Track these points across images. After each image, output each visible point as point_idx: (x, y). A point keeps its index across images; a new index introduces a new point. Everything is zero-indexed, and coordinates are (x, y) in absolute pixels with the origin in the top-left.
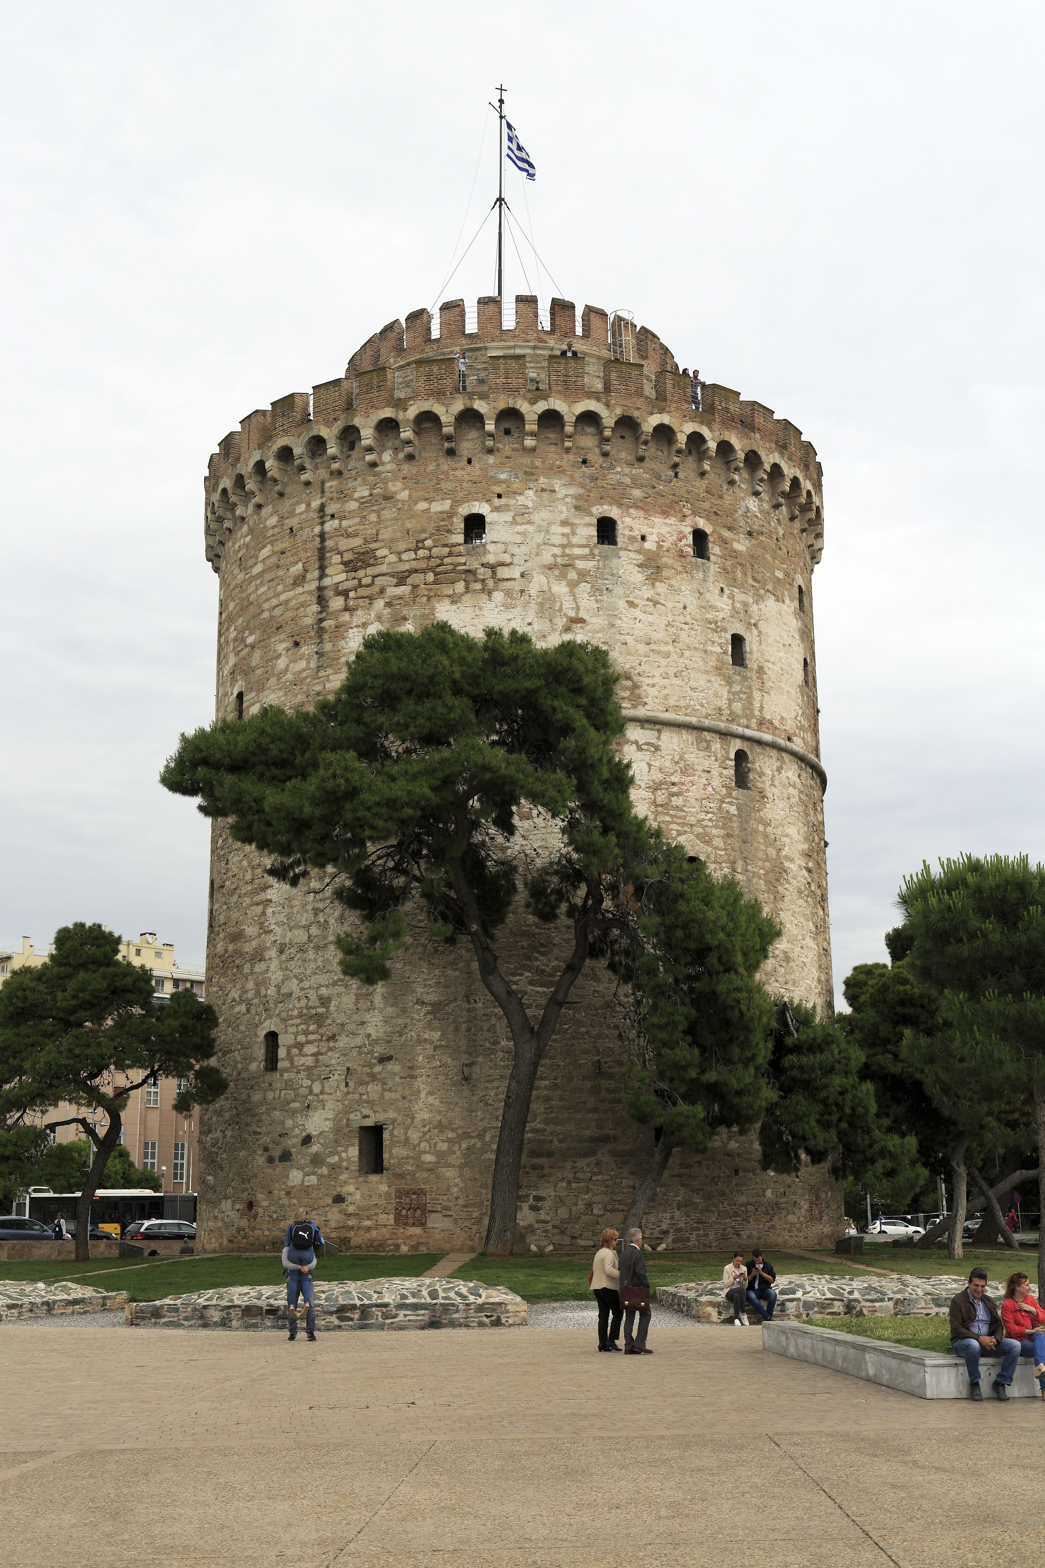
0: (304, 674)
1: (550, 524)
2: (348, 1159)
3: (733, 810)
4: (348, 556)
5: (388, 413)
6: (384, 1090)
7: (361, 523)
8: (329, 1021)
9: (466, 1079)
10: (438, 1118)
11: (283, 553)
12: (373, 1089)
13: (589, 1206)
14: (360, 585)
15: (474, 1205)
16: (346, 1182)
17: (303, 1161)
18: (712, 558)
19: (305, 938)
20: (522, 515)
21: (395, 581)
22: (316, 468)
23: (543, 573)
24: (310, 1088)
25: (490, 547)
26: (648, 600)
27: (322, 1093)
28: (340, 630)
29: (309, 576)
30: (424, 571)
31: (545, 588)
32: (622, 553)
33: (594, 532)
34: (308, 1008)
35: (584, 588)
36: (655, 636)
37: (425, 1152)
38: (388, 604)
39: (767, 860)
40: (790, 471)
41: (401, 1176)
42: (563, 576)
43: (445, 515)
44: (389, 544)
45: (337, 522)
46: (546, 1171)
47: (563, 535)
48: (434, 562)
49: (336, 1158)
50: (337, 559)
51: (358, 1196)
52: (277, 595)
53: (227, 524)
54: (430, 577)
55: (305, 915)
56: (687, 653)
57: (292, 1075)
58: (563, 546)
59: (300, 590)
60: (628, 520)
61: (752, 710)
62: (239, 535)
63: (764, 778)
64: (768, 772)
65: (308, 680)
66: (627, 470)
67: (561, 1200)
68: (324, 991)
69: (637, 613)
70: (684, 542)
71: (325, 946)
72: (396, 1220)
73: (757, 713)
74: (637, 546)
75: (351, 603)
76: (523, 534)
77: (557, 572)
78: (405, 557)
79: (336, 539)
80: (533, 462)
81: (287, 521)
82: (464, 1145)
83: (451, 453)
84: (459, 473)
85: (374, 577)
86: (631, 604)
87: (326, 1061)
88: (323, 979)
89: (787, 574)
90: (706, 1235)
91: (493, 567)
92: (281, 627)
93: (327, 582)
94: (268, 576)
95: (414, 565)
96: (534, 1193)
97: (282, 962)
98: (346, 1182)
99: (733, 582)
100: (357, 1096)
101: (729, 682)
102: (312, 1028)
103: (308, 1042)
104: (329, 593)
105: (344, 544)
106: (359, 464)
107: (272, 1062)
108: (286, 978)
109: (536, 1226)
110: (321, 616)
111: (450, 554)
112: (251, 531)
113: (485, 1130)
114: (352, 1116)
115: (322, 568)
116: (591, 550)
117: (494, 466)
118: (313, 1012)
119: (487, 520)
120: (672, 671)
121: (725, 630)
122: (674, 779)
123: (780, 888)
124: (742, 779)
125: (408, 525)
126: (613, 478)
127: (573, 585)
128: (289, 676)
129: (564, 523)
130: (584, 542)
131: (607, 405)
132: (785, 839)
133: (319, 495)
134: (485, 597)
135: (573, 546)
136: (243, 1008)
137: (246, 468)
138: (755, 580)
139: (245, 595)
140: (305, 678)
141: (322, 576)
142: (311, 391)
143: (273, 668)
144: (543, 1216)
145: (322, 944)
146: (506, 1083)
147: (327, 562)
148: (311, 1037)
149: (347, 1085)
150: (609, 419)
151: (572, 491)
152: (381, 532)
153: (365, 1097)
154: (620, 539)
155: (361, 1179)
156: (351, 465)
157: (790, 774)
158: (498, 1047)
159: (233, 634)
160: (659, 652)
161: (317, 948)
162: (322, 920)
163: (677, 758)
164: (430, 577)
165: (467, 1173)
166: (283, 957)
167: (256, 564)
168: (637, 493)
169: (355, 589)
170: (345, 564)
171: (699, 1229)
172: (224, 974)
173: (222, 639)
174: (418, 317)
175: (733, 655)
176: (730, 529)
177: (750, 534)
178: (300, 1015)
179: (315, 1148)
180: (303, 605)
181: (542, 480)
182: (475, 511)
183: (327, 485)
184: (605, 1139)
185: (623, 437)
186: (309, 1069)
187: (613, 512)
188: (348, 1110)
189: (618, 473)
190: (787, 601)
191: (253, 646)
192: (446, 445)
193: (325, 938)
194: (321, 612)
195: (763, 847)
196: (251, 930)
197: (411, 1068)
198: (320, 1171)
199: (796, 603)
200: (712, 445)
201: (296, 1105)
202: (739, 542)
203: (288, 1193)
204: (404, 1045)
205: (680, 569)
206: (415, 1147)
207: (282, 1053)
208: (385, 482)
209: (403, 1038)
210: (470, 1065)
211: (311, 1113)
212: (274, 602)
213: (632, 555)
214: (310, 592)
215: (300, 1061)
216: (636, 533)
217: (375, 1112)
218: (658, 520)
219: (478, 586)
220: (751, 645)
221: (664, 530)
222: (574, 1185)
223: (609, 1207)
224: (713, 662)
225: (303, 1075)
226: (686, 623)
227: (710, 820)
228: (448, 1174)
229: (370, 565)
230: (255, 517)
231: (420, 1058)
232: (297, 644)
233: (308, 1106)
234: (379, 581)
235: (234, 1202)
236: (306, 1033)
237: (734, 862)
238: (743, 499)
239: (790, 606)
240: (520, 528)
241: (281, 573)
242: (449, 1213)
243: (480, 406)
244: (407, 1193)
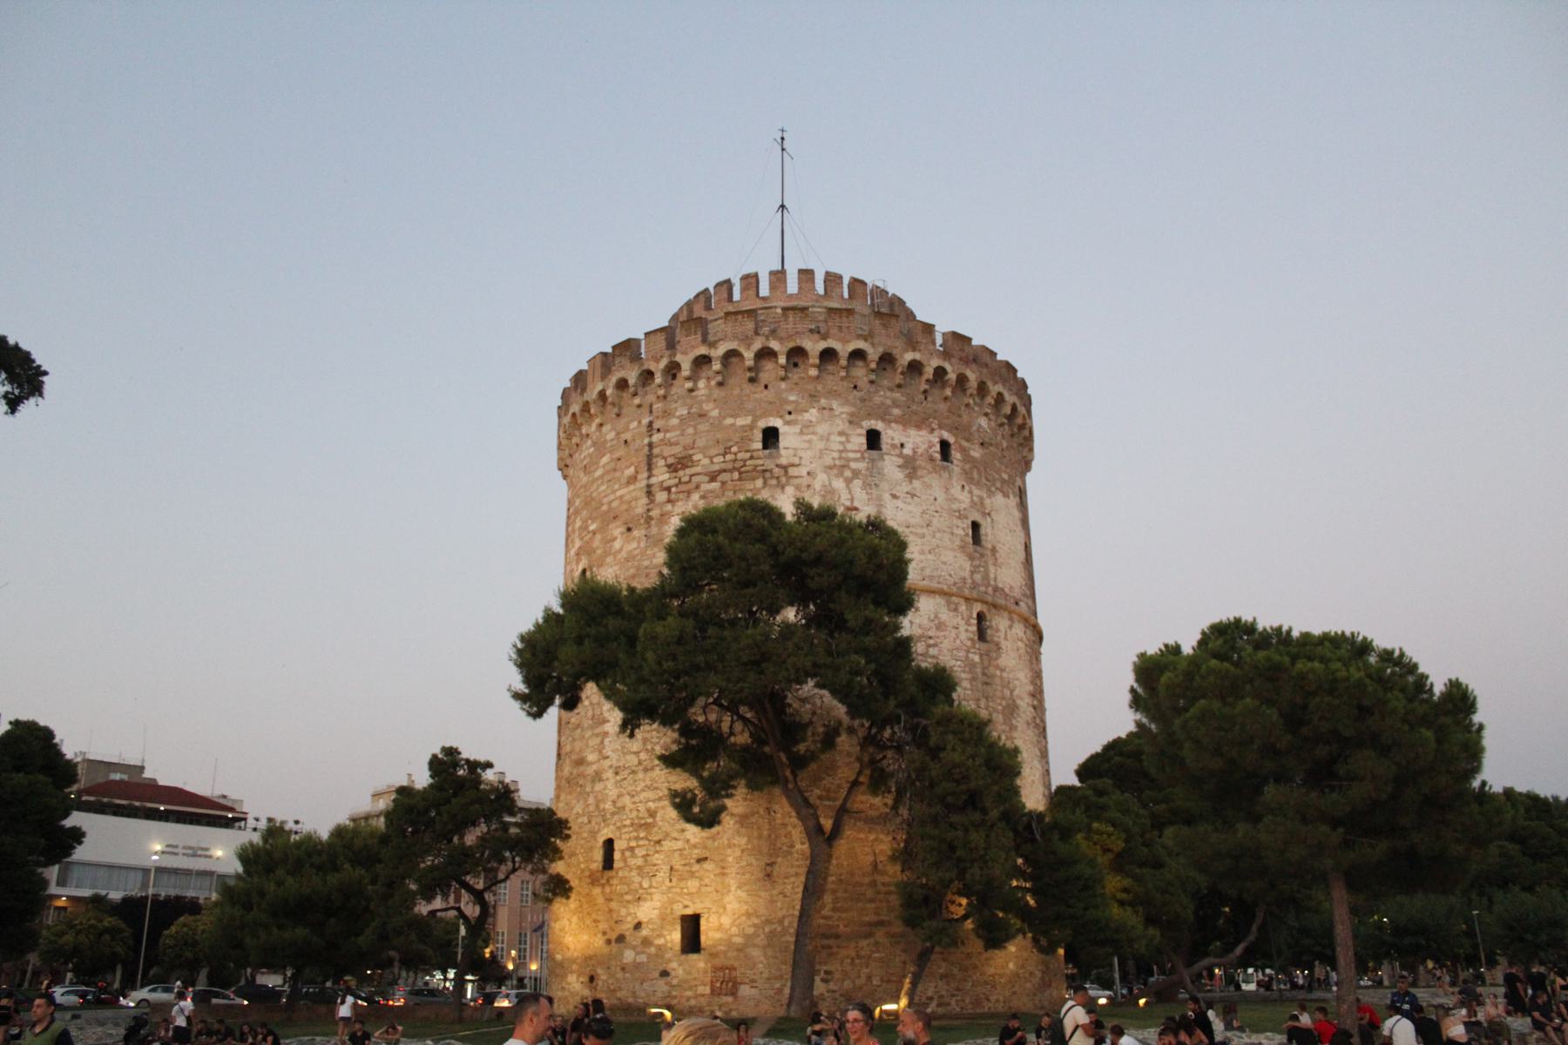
0: (636, 552)
1: (829, 434)
2: (672, 941)
3: (977, 658)
4: (671, 460)
5: (703, 350)
6: (701, 885)
7: (682, 435)
8: (656, 829)
9: (768, 875)
10: (745, 907)
11: (619, 459)
12: (693, 885)
13: (869, 978)
15: (776, 978)
18: (955, 462)
19: (636, 762)
20: (807, 428)
21: (707, 479)
22: (646, 393)
23: (825, 472)
24: (641, 884)
25: (783, 452)
26: (907, 493)
27: (651, 887)
28: (664, 517)
29: (639, 477)
30: (731, 471)
31: (827, 483)
32: (886, 457)
33: (863, 440)
34: (638, 817)
35: (857, 483)
36: (913, 521)
38: (703, 497)
39: (1003, 698)
40: (1010, 398)
41: (713, 955)
42: (841, 474)
43: (747, 428)
44: (703, 450)
45: (661, 435)
46: (835, 950)
47: (841, 443)
48: (738, 464)
51: (680, 971)
52: (614, 492)
53: (575, 440)
54: (736, 475)
56: (938, 535)
57: (626, 874)
58: (840, 451)
59: (632, 487)
60: (890, 432)
61: (988, 580)
62: (584, 447)
63: (999, 634)
64: (1002, 628)
66: (888, 394)
67: (845, 974)
68: (651, 804)
69: (899, 503)
70: (933, 449)
72: (712, 991)
73: (992, 583)
74: (897, 451)
75: (673, 496)
76: (809, 442)
77: (835, 471)
78: (715, 460)
80: (815, 388)
82: (767, 930)
83: (752, 380)
84: (757, 396)
85: (691, 476)
86: (894, 496)
88: (650, 795)
89: (1010, 476)
90: (963, 1001)
91: (785, 468)
93: (654, 480)
94: (607, 478)
95: (724, 466)
96: (825, 968)
97: (617, 782)
99: (970, 480)
100: (678, 890)
101: (971, 558)
102: (642, 835)
103: (638, 846)
104: (654, 489)
105: (667, 451)
107: (608, 863)
108: (620, 796)
109: (826, 994)
110: (650, 507)
112: (594, 444)
113: (784, 917)
114: (675, 907)
115: (650, 469)
116: (862, 454)
117: (786, 390)
118: (643, 822)
119: (781, 431)
120: (926, 548)
121: (967, 518)
122: (931, 633)
123: (1014, 721)
124: (982, 635)
125: (719, 436)
126: (877, 400)
127: (848, 481)
129: (841, 434)
130: (857, 448)
131: (873, 345)
132: (1017, 682)
134: (779, 490)
135: (848, 451)
136: (585, 820)
137: (592, 394)
138: (988, 480)
139: (588, 493)
141: (649, 477)
142: (642, 337)
143: (611, 548)
144: (832, 986)
146: (803, 879)
147: (653, 466)
148: (641, 843)
149: (671, 881)
150: (873, 354)
151: (847, 409)
152: (698, 440)
153: (685, 891)
154: (884, 446)
155: (683, 957)
156: (674, 390)
157: (1018, 631)
158: (794, 850)
159: (578, 524)
160: (916, 534)
162: (649, 747)
163: (932, 616)
164: (736, 475)
165: (770, 952)
166: (618, 778)
167: (597, 469)
168: (896, 411)
169: (676, 486)
170: (669, 466)
171: (956, 995)
172: (570, 793)
173: (570, 529)
174: (727, 285)
175: (973, 538)
176: (968, 441)
177: (982, 444)
178: (632, 825)
179: (644, 932)
180: (636, 499)
181: (823, 401)
182: (771, 425)
183: (655, 407)
184: (881, 923)
185: (885, 369)
186: (639, 868)
187: (879, 425)
188: (672, 902)
189: (881, 396)
190: (1011, 496)
191: (594, 533)
192: (749, 374)
195: (999, 688)
196: (591, 757)
197: (723, 868)
199: (1018, 499)
200: (952, 376)
201: (628, 897)
202: (974, 450)
203: (623, 969)
204: (717, 848)
205: (931, 469)
206: (727, 931)
207: (617, 855)
208: (701, 402)
209: (716, 844)
210: (771, 864)
211: (641, 903)
212: (612, 497)
213: (894, 458)
214: (641, 488)
215: (633, 862)
216: (897, 442)
217: (694, 903)
218: (912, 432)
219: (774, 482)
220: (986, 529)
221: (918, 440)
222: (857, 961)
223: (885, 979)
224: (958, 542)
226: (937, 512)
227: (959, 666)
229: (688, 467)
230: (598, 433)
231: (730, 859)
232: (629, 529)
234: (695, 479)
235: (578, 976)
236: (637, 838)
237: (979, 700)
238: (977, 418)
239: (1013, 501)
240: (809, 437)
241: (618, 474)
242: (755, 985)
243: (774, 345)
244: (722, 969)
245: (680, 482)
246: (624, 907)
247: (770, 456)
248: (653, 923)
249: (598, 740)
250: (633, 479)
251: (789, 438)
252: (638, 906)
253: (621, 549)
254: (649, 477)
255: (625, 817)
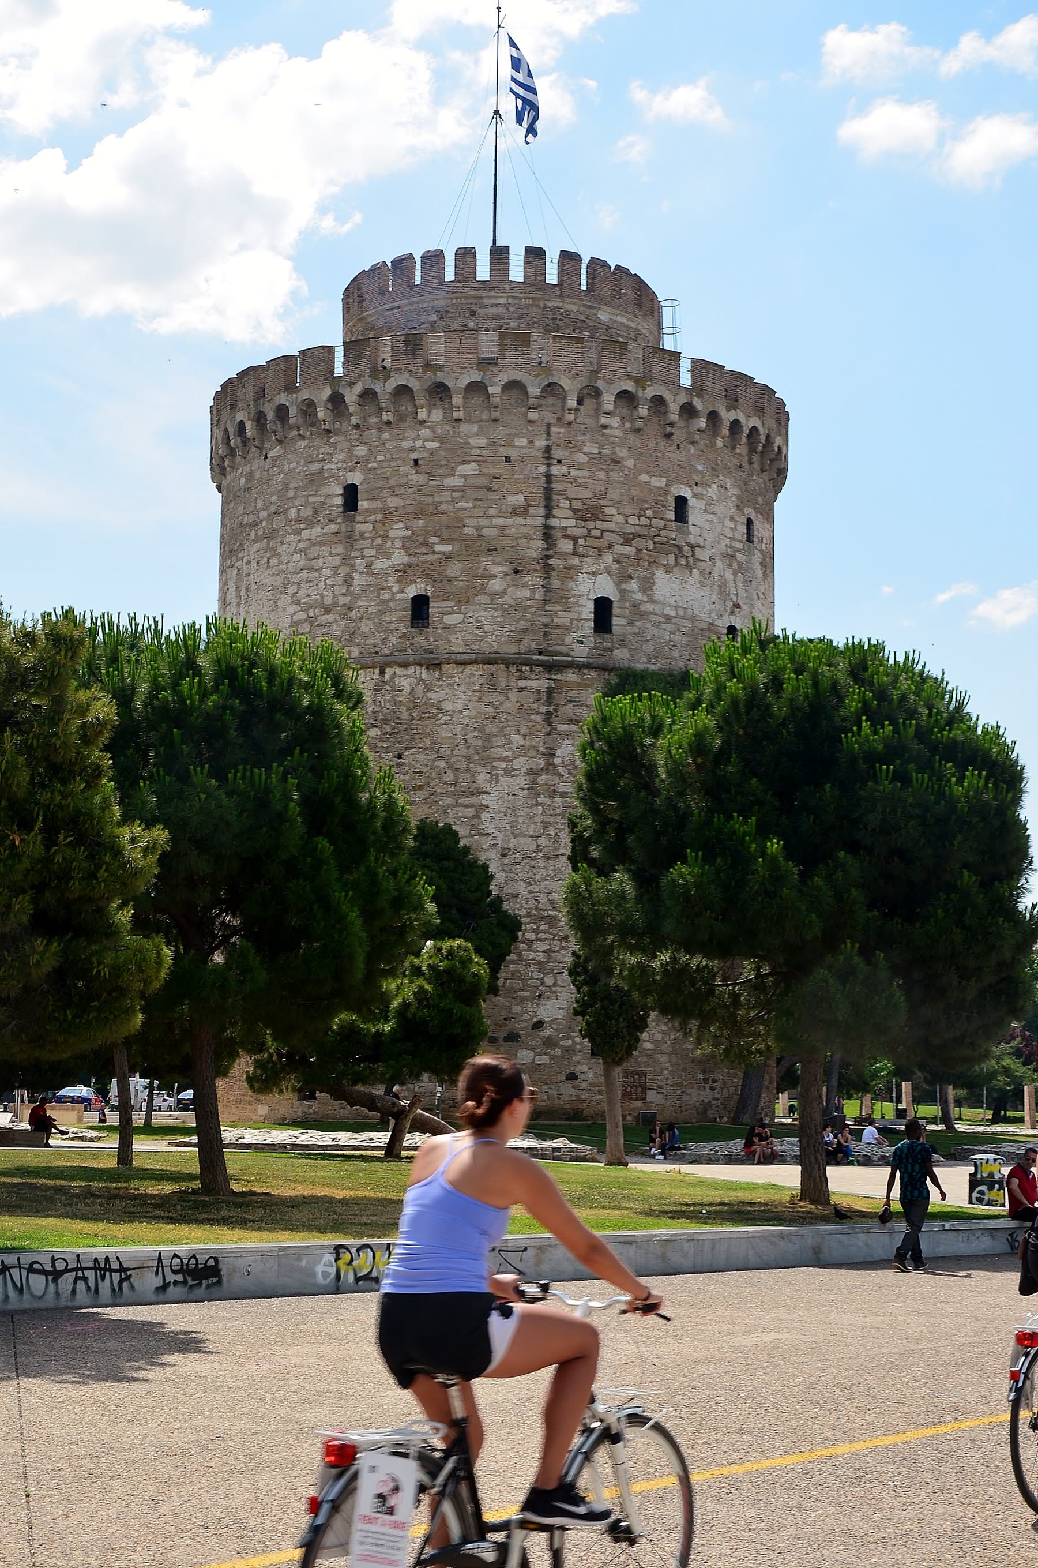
0: (529, 603)
4: (577, 505)
5: (629, 386)
11: (495, 478)
14: (589, 535)
16: (578, 1063)
17: (534, 1043)
19: (534, 847)
24: (542, 980)
25: (691, 529)
27: (554, 985)
28: (569, 573)
29: (532, 511)
34: (537, 908)
37: (646, 1041)
38: (616, 561)
42: (730, 565)
44: (617, 504)
45: (564, 469)
47: (731, 528)
48: (653, 532)
49: (570, 1042)
50: (565, 504)
55: (533, 826)
57: (520, 968)
59: (520, 521)
65: (534, 610)
71: (557, 857)
78: (631, 520)
79: (566, 485)
81: (501, 449)
83: (669, 436)
84: (671, 456)
87: (559, 958)
91: (692, 547)
92: (496, 549)
98: (578, 1063)
102: (542, 928)
106: (589, 421)
111: (665, 528)
118: (545, 914)
125: (634, 493)
128: (506, 599)
129: (732, 519)
133: (545, 437)
140: (530, 607)
141: (547, 516)
145: (552, 855)
148: (542, 936)
152: (610, 491)
155: (593, 1060)
161: (547, 858)
166: (506, 861)
167: (450, 475)
169: (584, 537)
170: (575, 511)
179: (547, 1033)
181: (721, 477)
183: (554, 430)
186: (539, 963)
187: (753, 516)
193: (557, 849)
194: (548, 549)
198: (553, 1052)
212: (483, 522)
214: (536, 527)
225: (532, 968)
228: (662, 1059)
232: (516, 572)
233: (540, 996)
236: (536, 931)
242: (662, 1091)
243: (698, 404)
245: (589, 535)
246: (517, 1004)
247: (678, 530)
248: (558, 1024)
249: (471, 812)
250: (523, 511)
251: (696, 514)
252: (538, 1005)
253: (504, 593)
254: (547, 516)
255: (518, 906)
